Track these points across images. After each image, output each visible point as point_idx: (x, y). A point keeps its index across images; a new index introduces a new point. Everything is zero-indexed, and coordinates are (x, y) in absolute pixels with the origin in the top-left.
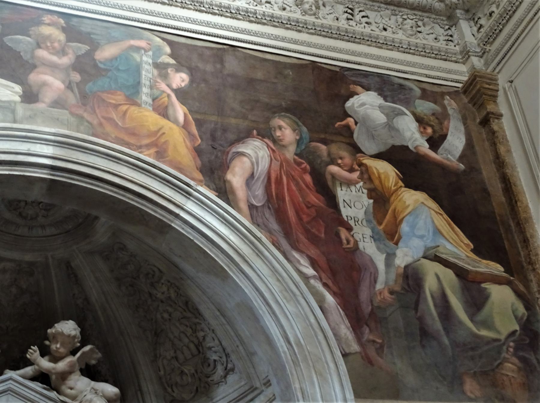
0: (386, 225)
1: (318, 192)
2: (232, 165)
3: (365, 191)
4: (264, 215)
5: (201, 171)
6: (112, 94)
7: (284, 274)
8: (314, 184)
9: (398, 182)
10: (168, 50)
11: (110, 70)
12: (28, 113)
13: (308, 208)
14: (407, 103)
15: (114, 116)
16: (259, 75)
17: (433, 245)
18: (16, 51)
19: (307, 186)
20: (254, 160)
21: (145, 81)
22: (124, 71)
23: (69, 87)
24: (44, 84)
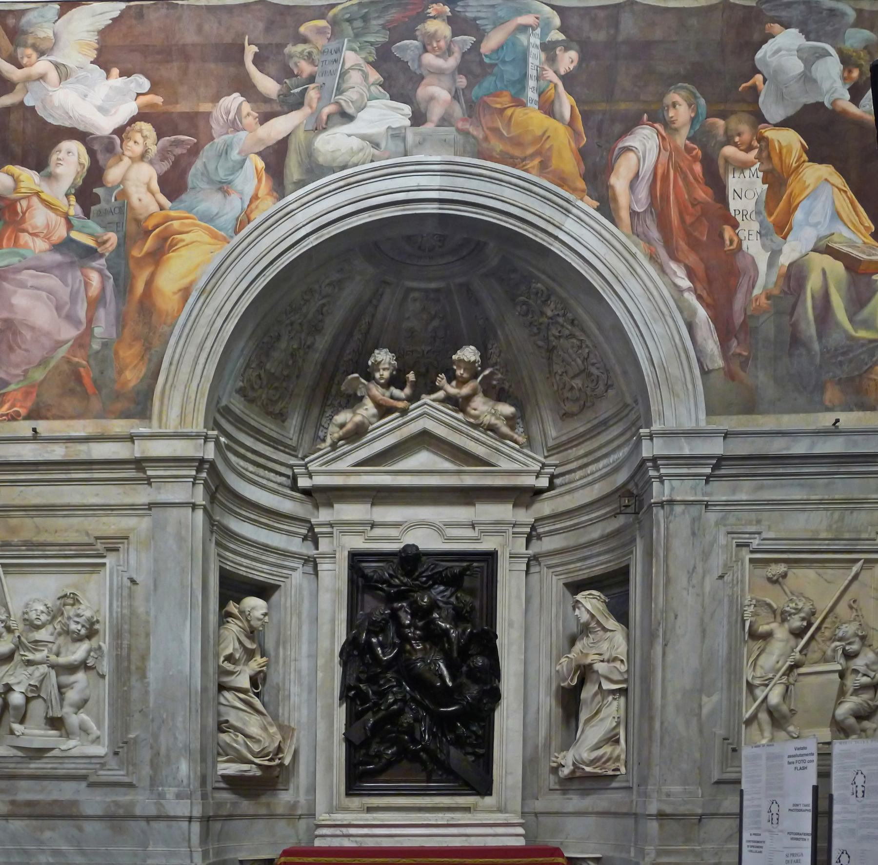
0: (777, 216)
1: (706, 184)
2: (616, 166)
3: (761, 174)
4: (646, 222)
5: (585, 178)
6: (498, 96)
7: (655, 293)
8: (703, 175)
9: (801, 156)
10: (557, 21)
11: (496, 65)
12: (418, 139)
13: (693, 205)
14: (835, 38)
15: (500, 125)
16: (658, 34)
17: (828, 233)
18: (403, 61)
20: (641, 154)
21: (532, 72)
22: (510, 62)
23: (455, 97)
24: (432, 98)
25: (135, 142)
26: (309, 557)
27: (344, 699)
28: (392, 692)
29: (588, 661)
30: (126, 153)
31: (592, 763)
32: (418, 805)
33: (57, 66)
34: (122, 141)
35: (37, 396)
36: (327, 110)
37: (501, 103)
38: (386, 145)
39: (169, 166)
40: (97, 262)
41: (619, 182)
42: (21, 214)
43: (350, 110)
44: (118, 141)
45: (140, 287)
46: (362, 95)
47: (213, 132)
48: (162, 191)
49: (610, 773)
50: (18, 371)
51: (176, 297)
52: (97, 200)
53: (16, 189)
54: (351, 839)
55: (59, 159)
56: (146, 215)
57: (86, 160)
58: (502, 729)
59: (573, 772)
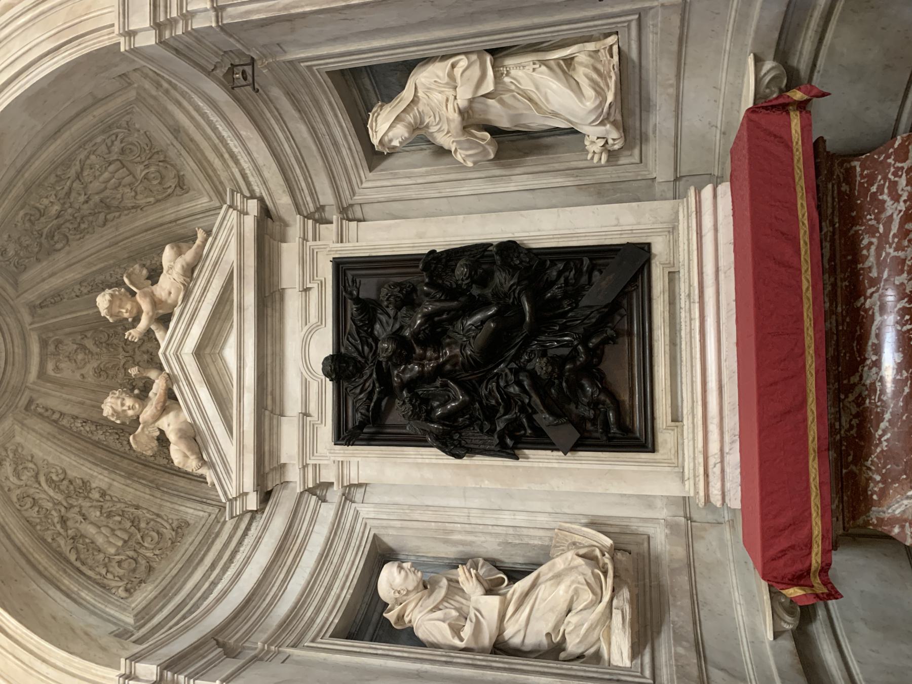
26: (343, 495)
27: (517, 452)
28: (505, 387)
29: (456, 117)
31: (600, 93)
32: (667, 348)
49: (616, 58)
54: (726, 449)
58: (554, 237)
59: (614, 124)
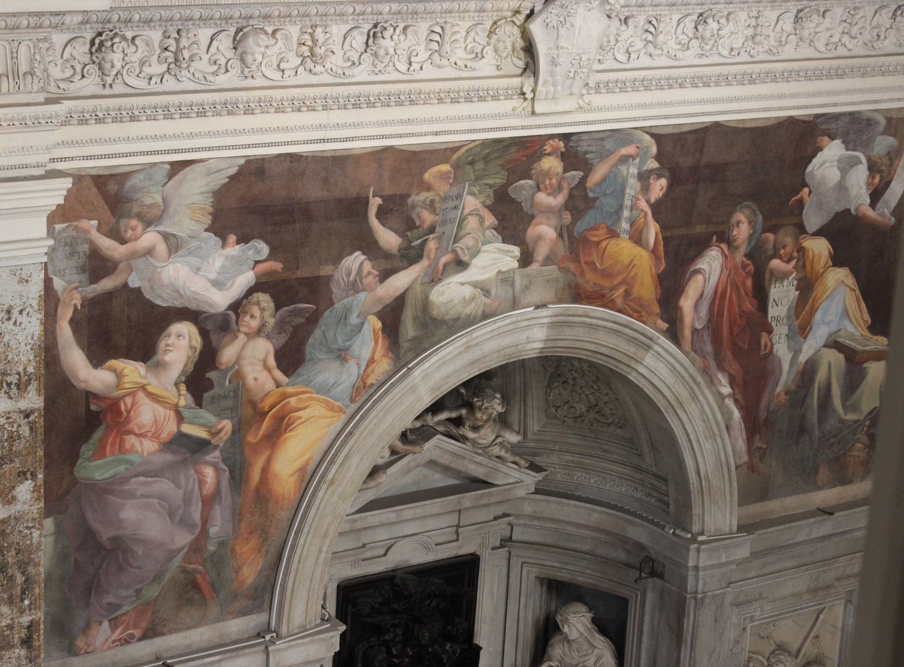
1: (755, 296)
2: (687, 288)
3: (795, 282)
8: (753, 289)
15: (595, 258)
17: (837, 329)
19: (746, 293)
20: (707, 275)
21: (627, 202)
23: (560, 235)
24: (540, 237)
25: (252, 316)
30: (242, 329)
33: (166, 236)
34: (238, 316)
35: (153, 613)
36: (443, 260)
37: (598, 236)
38: (496, 291)
39: (286, 339)
40: (211, 455)
41: (687, 303)
42: (125, 414)
43: (465, 258)
44: (233, 317)
45: (256, 475)
46: (477, 240)
47: (333, 296)
48: (280, 366)
50: (131, 592)
51: (292, 480)
52: (210, 385)
53: (118, 386)
55: (167, 345)
56: (262, 395)
57: (197, 341)
